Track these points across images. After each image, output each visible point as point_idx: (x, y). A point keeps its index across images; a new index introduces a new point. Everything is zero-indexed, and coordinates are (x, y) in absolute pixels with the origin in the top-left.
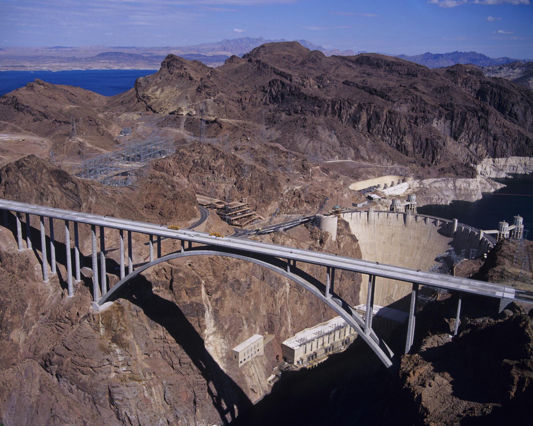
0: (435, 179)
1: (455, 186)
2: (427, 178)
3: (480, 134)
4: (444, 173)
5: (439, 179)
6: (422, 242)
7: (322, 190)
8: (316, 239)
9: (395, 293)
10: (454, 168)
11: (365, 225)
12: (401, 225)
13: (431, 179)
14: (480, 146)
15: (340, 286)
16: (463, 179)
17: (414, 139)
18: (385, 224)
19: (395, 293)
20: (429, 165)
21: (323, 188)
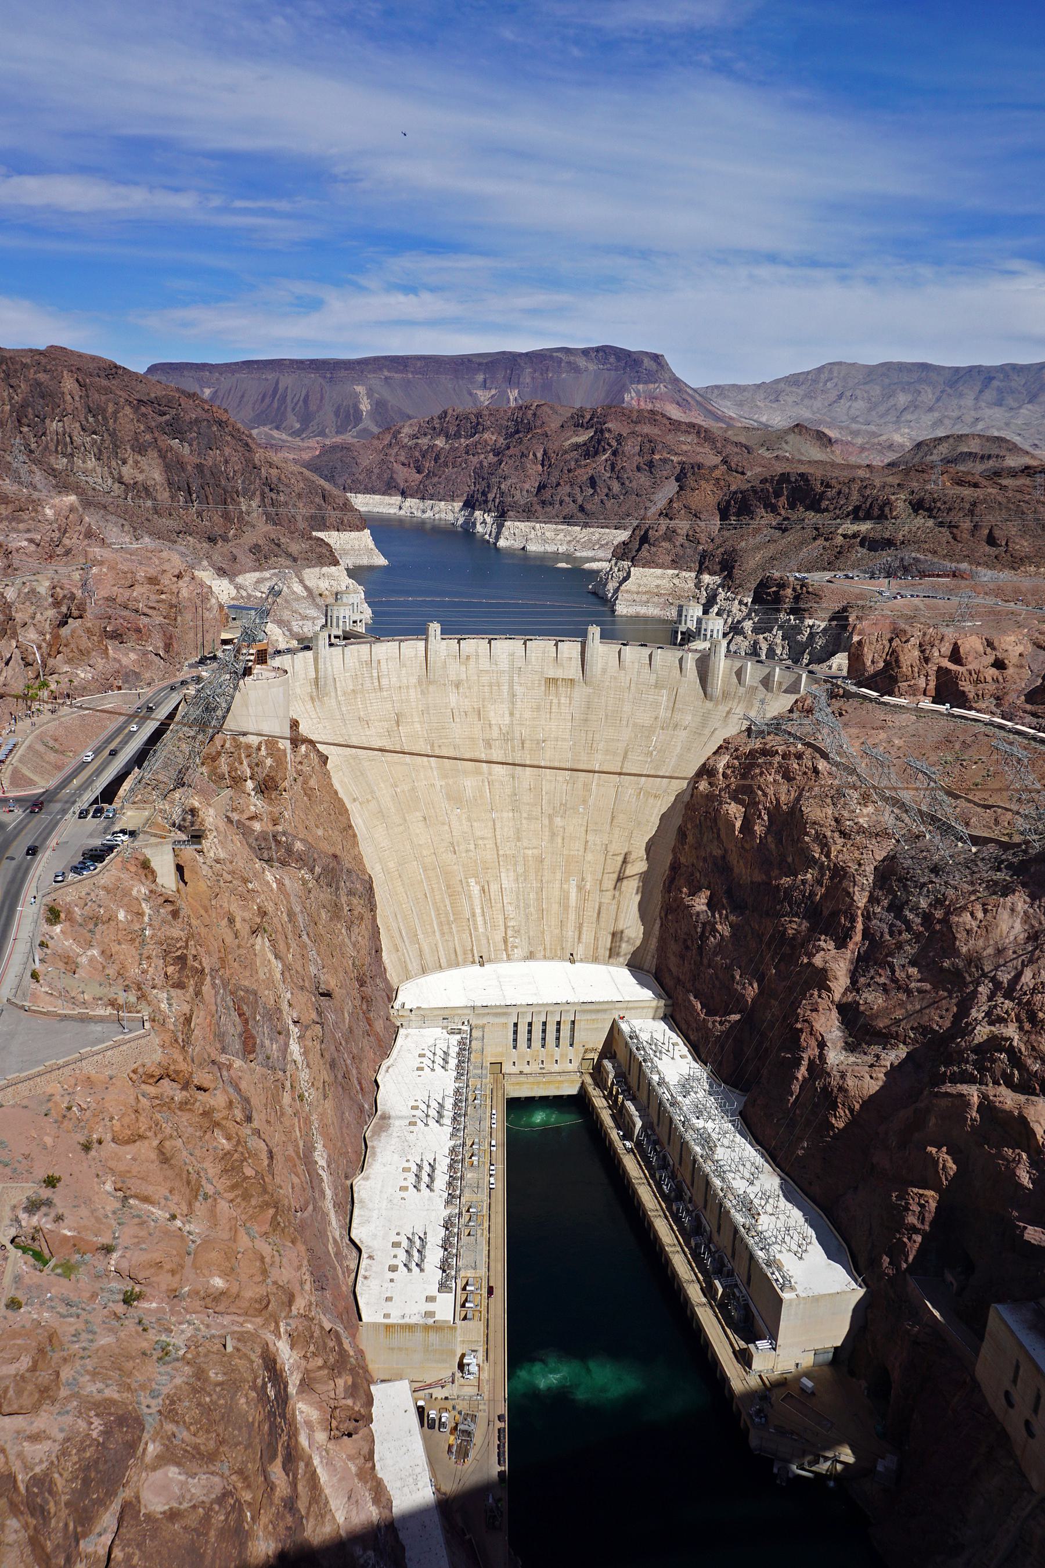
1: (306, 587)
2: (240, 573)
5: (267, 574)
6: (493, 722)
7: (153, 581)
8: (237, 781)
9: (478, 911)
10: (279, 545)
11: (312, 699)
12: (413, 680)
13: (248, 575)
15: (354, 945)
17: (168, 468)
18: (368, 685)
19: (478, 911)
20: (226, 540)
21: (152, 572)
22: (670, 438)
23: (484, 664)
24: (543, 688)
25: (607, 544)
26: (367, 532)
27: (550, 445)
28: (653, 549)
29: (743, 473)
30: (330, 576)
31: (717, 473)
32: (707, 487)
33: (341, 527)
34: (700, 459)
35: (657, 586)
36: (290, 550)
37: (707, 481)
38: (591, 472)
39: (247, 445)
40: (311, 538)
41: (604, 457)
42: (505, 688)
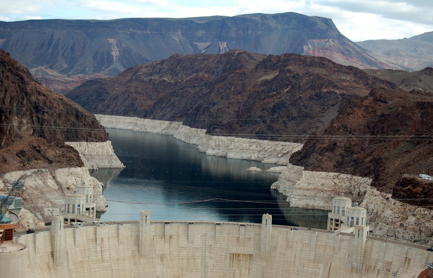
0: (21, 173)
1: (57, 183)
2: (8, 171)
3: (23, 99)
4: (29, 160)
5: (28, 172)
10: (39, 151)
11: (49, 267)
14: (25, 121)
16: (66, 169)
22: (334, 77)
23: (183, 242)
24: (228, 261)
25: (288, 153)
26: (109, 143)
27: (247, 81)
28: (320, 157)
29: (385, 102)
30: (76, 175)
31: (366, 103)
32: (360, 112)
33: (89, 139)
34: (356, 92)
35: (323, 185)
36: (47, 155)
37: (359, 107)
38: (276, 101)
39: (22, 78)
40: (63, 146)
41: (286, 90)
42: (199, 261)
